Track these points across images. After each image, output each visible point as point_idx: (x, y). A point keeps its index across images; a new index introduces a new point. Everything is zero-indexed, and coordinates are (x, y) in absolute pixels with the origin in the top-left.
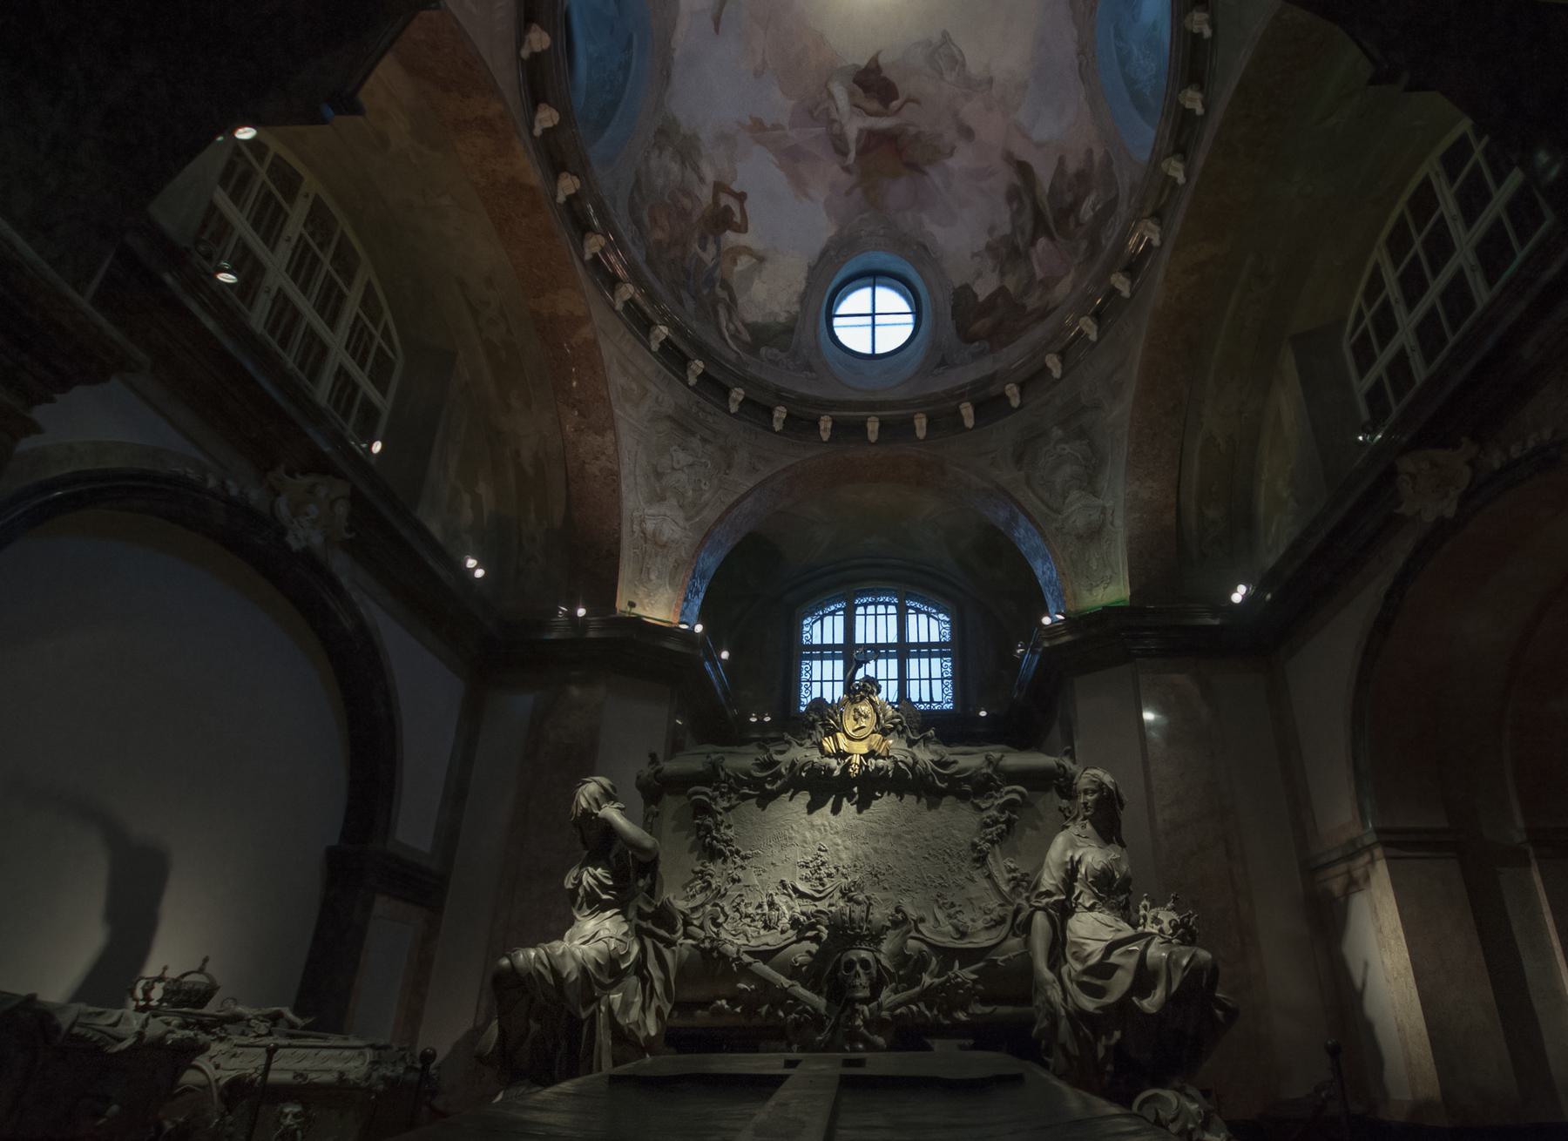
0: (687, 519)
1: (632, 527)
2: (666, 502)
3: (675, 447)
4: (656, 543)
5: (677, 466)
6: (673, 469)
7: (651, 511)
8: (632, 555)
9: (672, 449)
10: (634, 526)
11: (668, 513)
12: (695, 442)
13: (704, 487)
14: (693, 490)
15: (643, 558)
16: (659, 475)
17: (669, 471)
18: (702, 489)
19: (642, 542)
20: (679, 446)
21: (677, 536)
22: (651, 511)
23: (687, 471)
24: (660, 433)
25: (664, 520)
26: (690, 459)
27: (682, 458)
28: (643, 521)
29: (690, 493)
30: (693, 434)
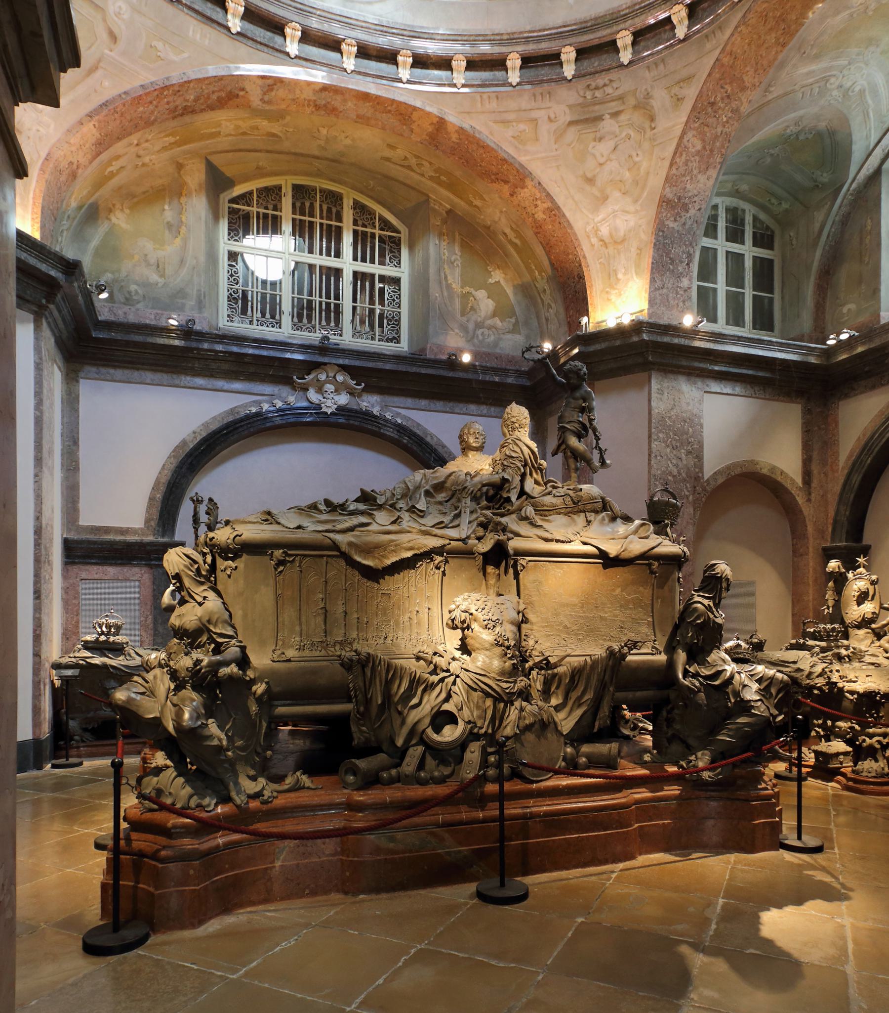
0: (636, 201)
1: (590, 241)
2: (610, 200)
3: (593, 144)
4: (615, 242)
5: (602, 160)
6: (601, 164)
7: (601, 217)
8: (598, 266)
9: (590, 149)
10: (592, 240)
11: (616, 208)
12: (608, 125)
13: (637, 159)
14: (629, 170)
15: (609, 264)
16: (590, 181)
17: (598, 170)
18: (635, 163)
19: (604, 249)
20: (595, 140)
21: (632, 224)
22: (601, 217)
23: (613, 157)
24: (572, 143)
25: (615, 216)
26: (611, 144)
27: (603, 149)
28: (596, 231)
29: (627, 174)
30: (600, 118)
